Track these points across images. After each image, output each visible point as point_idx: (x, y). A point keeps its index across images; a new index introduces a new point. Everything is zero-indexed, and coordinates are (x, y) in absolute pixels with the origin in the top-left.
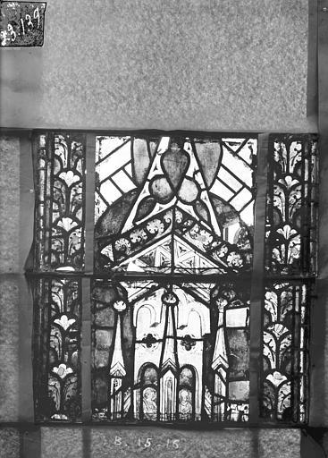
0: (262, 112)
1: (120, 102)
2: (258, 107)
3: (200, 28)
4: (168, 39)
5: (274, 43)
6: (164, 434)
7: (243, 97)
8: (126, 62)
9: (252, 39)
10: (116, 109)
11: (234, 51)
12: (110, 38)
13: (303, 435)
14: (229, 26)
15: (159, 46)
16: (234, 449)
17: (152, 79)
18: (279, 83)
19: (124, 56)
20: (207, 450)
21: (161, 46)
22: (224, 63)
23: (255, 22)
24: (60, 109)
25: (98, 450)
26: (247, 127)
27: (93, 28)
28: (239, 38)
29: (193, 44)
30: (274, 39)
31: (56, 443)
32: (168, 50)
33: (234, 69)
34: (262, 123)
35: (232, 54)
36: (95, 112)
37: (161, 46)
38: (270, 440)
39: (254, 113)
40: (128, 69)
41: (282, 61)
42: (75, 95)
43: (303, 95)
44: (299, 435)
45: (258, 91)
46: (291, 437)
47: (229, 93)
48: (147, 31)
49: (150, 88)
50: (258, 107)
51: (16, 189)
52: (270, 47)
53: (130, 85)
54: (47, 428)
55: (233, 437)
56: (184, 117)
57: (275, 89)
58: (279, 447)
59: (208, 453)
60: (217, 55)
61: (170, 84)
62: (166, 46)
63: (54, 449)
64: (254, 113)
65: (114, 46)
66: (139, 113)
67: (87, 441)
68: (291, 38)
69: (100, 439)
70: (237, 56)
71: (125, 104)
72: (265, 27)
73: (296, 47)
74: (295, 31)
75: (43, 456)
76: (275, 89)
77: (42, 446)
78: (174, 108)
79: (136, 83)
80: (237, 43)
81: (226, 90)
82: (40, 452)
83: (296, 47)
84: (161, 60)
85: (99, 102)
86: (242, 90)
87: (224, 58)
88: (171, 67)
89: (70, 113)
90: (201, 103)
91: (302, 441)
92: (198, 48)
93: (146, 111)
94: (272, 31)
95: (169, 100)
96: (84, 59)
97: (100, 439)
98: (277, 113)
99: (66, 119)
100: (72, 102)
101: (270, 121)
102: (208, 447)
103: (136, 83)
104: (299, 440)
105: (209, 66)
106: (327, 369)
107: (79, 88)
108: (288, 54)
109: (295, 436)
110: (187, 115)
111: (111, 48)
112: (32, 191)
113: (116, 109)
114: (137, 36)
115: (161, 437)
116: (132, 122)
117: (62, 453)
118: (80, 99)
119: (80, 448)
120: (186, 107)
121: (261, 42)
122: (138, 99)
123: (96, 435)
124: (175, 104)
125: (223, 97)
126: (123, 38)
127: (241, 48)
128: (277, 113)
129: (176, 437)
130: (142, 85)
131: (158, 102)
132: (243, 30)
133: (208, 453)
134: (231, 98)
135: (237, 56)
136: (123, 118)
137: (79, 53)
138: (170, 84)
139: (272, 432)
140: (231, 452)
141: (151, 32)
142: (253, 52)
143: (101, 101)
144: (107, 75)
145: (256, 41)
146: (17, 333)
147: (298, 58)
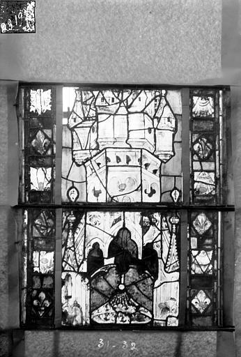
0: (180, 69)
1: (75, 60)
2: (177, 66)
3: (133, 8)
4: (110, 16)
5: (188, 19)
6: (116, 337)
7: (166, 59)
8: (78, 32)
9: (172, 16)
10: (71, 65)
11: (160, 24)
12: (66, 15)
13: (219, 337)
14: (155, 7)
15: (102, 21)
16: (168, 348)
17: (98, 44)
18: (192, 48)
19: (77, 28)
20: (147, 348)
21: (105, 21)
22: (151, 34)
23: (174, 3)
24: (29, 65)
25: (68, 348)
26: (169, 80)
27: (54, 6)
28: (162, 15)
29: (128, 20)
30: (188, 16)
31: (36, 343)
32: (110, 25)
33: (159, 37)
34: (180, 77)
35: (156, 28)
36: (55, 67)
37: (105, 21)
38: (195, 341)
39: (174, 70)
40: (80, 37)
41: (194, 32)
42: (40, 55)
43: (210, 57)
44: (216, 337)
45: (177, 54)
46: (210, 339)
47: (155, 56)
48: (94, 11)
49: (97, 50)
50: (177, 66)
51: (5, 143)
52: (185, 22)
53: (82, 48)
54: (30, 332)
55: (167, 339)
56: (122, 72)
57: (189, 53)
58: (200, 346)
59: (149, 350)
60: (146, 29)
61: (111, 48)
62: (108, 21)
63: (35, 347)
64: (174, 70)
65: (70, 21)
66: (88, 68)
67: (56, 342)
68: (201, 15)
69: (69, 340)
70: (161, 29)
71: (77, 62)
72: (181, 7)
73: (205, 21)
74: (204, 10)
75: (26, 353)
76: (189, 53)
77: (26, 346)
78: (115, 66)
79: (86, 47)
80: (161, 20)
81: (154, 53)
82: (24, 350)
83: (205, 21)
84: (105, 31)
85: (58, 60)
86: (165, 53)
87: (151, 31)
88: (112, 37)
89: (37, 68)
90: (135, 63)
91: (218, 342)
92: (132, 23)
93: (94, 67)
94: (187, 10)
95: (111, 60)
96: (47, 30)
97: (69, 340)
98: (191, 69)
99: (33, 72)
100: (38, 59)
101: (186, 76)
102: (148, 346)
103: (86, 47)
104: (216, 341)
105: (140, 37)
106: (239, 288)
107: (43, 49)
108: (198, 27)
109: (212, 338)
110: (124, 71)
111: (67, 22)
112: (17, 144)
113: (71, 65)
114: (87, 13)
115: (114, 339)
116: (83, 76)
117: (41, 350)
118: (44, 58)
119: (53, 347)
120: (123, 64)
121: (179, 18)
122: (88, 58)
123: (64, 336)
124: (115, 63)
125: (151, 59)
126: (76, 14)
127: (164, 23)
128: (191, 69)
129: (125, 339)
130: (90, 48)
131: (103, 61)
132: (165, 9)
133: (149, 350)
134: (157, 59)
135: (161, 29)
136: (77, 73)
137: (43, 24)
138: (111, 48)
139: (197, 335)
140: (166, 350)
141: (97, 11)
142: (172, 26)
143: (60, 59)
144: (64, 41)
145: (175, 18)
146: (7, 250)
147: (206, 29)
